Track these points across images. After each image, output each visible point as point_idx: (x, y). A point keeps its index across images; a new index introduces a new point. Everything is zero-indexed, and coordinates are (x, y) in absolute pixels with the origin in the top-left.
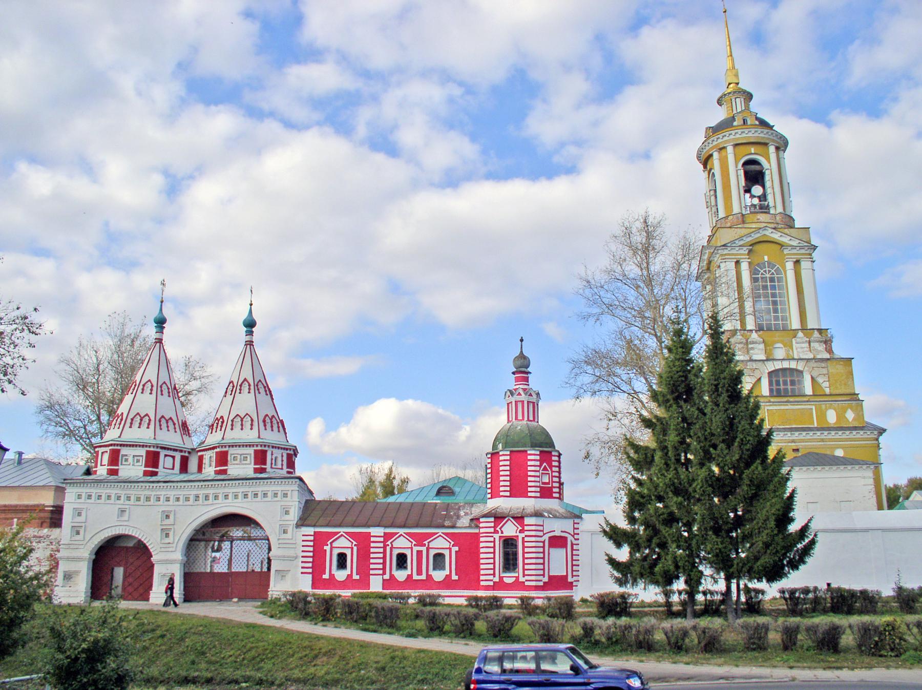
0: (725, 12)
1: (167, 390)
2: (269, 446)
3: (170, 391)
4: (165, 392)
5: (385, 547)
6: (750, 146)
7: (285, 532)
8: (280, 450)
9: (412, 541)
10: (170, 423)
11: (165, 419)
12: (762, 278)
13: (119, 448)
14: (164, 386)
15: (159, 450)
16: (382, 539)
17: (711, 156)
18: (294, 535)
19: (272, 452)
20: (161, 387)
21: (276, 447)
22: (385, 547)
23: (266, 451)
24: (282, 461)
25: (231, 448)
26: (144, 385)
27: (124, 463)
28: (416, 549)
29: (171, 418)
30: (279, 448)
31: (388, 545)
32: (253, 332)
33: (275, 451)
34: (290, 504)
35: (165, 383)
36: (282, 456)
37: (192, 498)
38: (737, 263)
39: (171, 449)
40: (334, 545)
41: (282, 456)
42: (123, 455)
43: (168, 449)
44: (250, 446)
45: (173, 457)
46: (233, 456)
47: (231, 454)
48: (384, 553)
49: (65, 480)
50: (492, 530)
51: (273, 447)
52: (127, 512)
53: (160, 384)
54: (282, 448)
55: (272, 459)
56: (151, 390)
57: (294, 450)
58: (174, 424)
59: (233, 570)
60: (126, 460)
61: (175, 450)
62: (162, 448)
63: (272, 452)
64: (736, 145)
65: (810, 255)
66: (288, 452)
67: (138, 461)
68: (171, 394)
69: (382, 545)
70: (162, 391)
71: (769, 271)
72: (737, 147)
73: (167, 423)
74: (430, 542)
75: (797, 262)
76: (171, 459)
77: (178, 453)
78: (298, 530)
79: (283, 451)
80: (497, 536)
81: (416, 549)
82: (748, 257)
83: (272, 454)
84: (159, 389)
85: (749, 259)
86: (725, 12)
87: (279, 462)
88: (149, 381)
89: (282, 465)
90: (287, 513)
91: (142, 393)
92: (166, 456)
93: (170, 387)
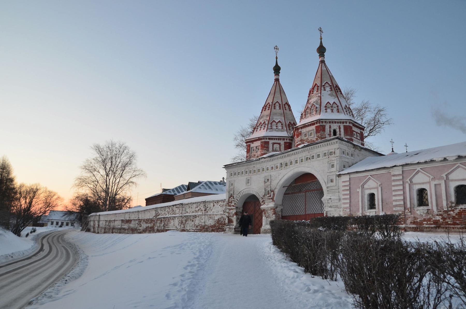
1: (279, 106)
2: (325, 122)
3: (281, 106)
4: (277, 107)
5: (403, 185)
7: (332, 181)
8: (337, 124)
9: (431, 176)
10: (279, 125)
11: (276, 122)
13: (249, 143)
14: (277, 104)
15: (268, 140)
18: (337, 183)
19: (330, 126)
20: (275, 105)
21: (332, 122)
22: (403, 185)
23: (325, 126)
24: (340, 131)
25: (302, 129)
26: (266, 106)
27: (253, 152)
28: (433, 183)
29: (279, 121)
30: (335, 122)
31: (407, 182)
32: (324, 55)
33: (332, 125)
34: (333, 159)
35: (277, 102)
36: (340, 128)
37: (279, 165)
39: (276, 139)
40: (366, 186)
41: (340, 128)
42: (252, 148)
43: (274, 139)
44: (313, 124)
45: (279, 144)
46: (304, 134)
47: (303, 133)
49: (225, 166)
51: (330, 122)
52: (250, 180)
53: (274, 103)
54: (338, 123)
55: (330, 131)
56: (269, 108)
57: (350, 123)
58: (282, 125)
59: (307, 213)
60: (254, 150)
61: (281, 139)
62: (269, 139)
63: (330, 126)
66: (345, 124)
67: (258, 149)
68: (281, 108)
70: (275, 107)
73: (277, 124)
74: (449, 174)
76: (278, 146)
77: (282, 141)
78: (339, 178)
79: (339, 124)
81: (433, 183)
83: (330, 127)
84: (273, 106)
87: (338, 133)
88: (269, 103)
89: (340, 134)
90: (333, 166)
91: (265, 111)
92: (274, 144)
93: (281, 103)
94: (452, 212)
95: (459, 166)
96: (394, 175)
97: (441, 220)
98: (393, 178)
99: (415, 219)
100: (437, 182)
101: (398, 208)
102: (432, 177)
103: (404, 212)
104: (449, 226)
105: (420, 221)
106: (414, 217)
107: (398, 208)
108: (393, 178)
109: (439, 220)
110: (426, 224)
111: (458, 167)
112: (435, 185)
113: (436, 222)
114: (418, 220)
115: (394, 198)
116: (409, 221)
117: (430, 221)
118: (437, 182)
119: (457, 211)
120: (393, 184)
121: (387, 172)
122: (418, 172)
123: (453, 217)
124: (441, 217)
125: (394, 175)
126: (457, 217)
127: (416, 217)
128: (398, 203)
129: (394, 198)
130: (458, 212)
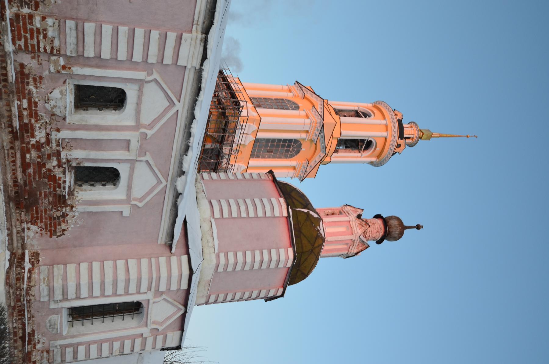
0: (467, 137)
6: (381, 150)
12: (290, 145)
16: (168, 60)
17: (384, 118)
28: (133, 137)
38: (307, 132)
48: (130, 62)
50: (163, 288)
64: (386, 139)
65: (297, 176)
69: (152, 59)
71: (293, 150)
72: (383, 139)
75: (294, 168)
80: (150, 296)
81: (133, 137)
82: (309, 139)
85: (308, 140)
86: (467, 137)
94: (55, 163)
95: (162, 183)
96: (180, 38)
97: (33, 141)
98: (172, 37)
99: (35, 80)
100: (134, 145)
101: (71, 39)
102: (150, 133)
103: (59, 54)
104: (18, 155)
105: (30, 92)
106: (41, 78)
107: (71, 39)
108: (172, 37)
109: (33, 136)
110: (19, 107)
111: (160, 182)
112: (129, 141)
113: (27, 129)
114: (31, 87)
115: (107, 29)
116: (26, 59)
117: (30, 115)
118: (134, 145)
119: (58, 172)
120: (155, 35)
121: (196, 18)
122: (172, 104)
123: (44, 166)
124: (43, 140)
125: (180, 38)
126: (44, 170)
127: (40, 83)
128: (89, 39)
129: (107, 29)
130: (55, 176)
